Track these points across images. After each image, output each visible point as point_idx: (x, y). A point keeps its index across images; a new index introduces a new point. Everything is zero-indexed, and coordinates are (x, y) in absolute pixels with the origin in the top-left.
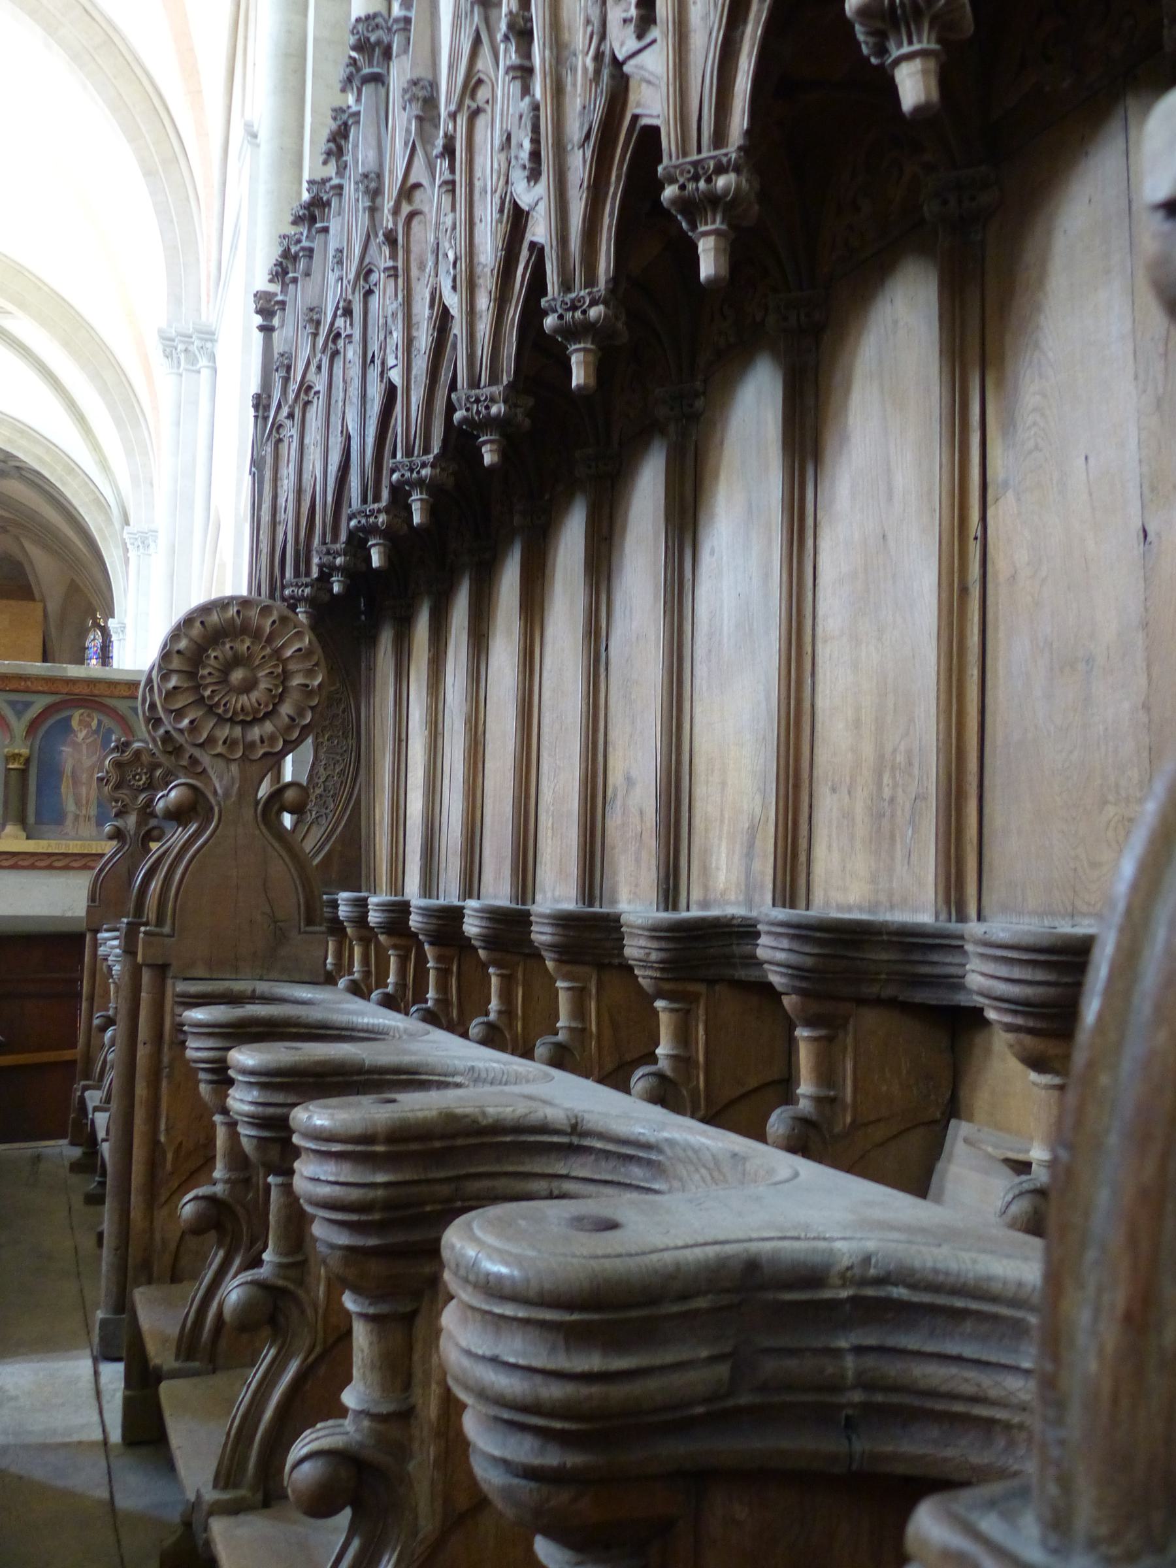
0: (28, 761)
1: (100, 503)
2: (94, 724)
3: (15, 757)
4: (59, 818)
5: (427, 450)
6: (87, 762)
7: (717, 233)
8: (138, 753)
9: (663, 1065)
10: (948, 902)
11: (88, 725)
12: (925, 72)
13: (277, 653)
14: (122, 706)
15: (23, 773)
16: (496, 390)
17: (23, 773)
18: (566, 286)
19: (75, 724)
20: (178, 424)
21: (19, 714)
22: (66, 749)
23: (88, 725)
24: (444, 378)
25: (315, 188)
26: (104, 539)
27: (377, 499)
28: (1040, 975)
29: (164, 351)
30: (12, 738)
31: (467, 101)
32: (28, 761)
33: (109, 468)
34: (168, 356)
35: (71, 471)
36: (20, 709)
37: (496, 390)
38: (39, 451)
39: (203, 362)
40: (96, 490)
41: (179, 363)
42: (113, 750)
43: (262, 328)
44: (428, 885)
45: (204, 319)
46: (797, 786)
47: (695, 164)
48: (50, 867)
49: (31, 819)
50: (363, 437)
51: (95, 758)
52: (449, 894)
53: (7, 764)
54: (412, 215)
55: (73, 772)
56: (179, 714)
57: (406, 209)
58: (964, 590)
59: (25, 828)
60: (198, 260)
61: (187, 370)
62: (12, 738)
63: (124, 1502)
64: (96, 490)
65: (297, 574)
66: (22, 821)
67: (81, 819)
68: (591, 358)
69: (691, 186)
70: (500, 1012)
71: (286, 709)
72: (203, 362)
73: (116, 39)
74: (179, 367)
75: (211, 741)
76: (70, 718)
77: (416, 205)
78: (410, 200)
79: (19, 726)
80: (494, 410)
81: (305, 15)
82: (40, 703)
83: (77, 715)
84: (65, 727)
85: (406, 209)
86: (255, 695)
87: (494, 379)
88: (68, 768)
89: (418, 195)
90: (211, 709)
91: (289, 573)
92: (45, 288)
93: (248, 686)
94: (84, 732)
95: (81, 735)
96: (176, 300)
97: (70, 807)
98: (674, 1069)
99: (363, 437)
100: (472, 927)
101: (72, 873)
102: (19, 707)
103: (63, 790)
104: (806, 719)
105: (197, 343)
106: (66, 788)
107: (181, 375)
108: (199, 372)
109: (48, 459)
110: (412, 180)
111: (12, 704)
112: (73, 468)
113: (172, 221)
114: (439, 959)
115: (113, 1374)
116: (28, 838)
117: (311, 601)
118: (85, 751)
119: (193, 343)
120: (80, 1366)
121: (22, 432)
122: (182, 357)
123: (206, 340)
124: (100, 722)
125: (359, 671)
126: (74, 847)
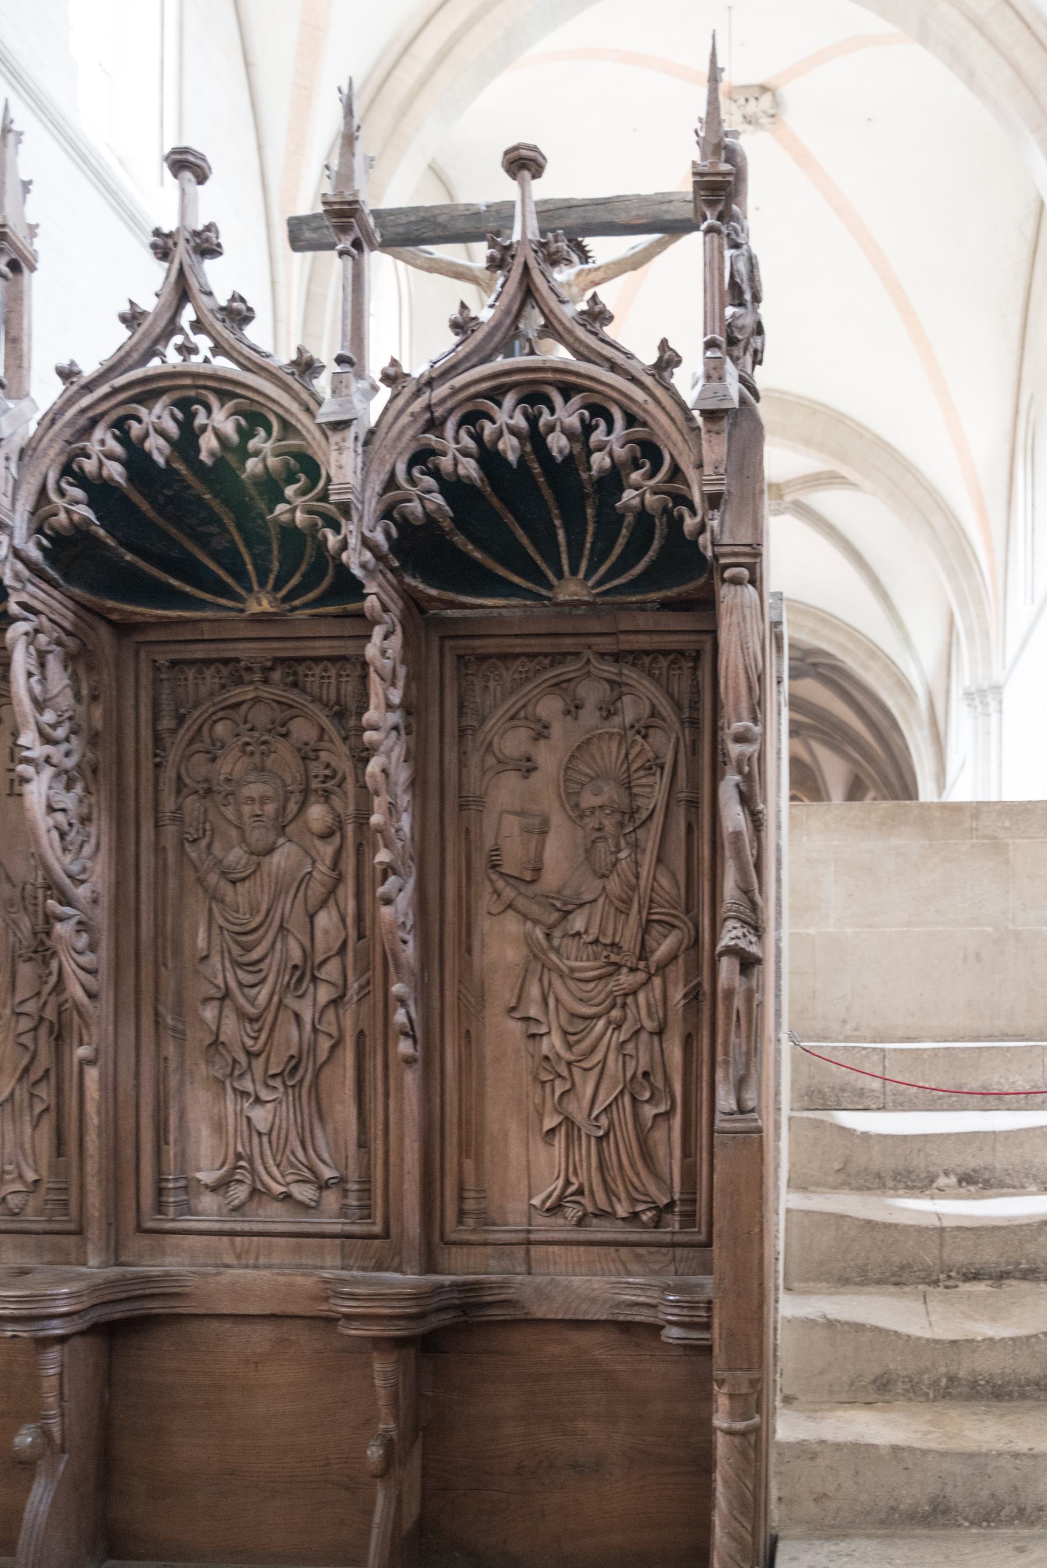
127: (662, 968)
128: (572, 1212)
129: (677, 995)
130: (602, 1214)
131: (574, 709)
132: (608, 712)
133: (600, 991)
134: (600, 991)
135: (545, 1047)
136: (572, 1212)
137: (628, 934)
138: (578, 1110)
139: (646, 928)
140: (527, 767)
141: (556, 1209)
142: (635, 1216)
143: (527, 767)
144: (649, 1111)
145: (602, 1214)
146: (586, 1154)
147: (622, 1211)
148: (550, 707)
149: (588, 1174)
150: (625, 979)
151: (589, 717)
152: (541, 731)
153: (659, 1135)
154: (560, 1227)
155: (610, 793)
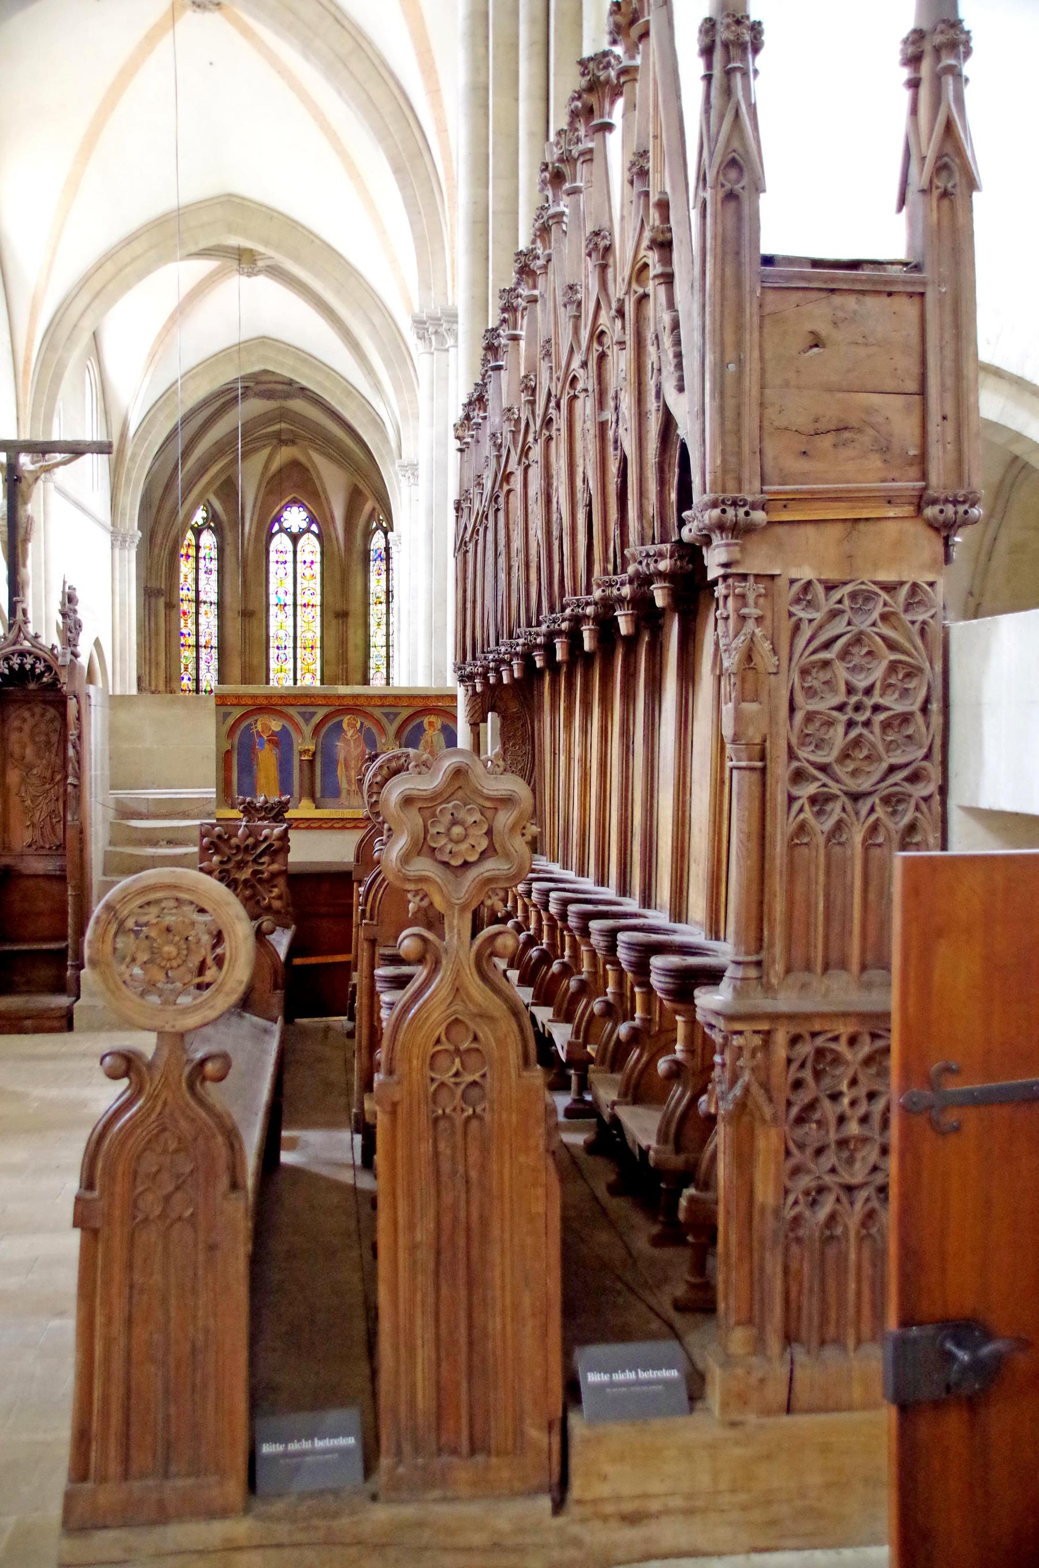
0: (314, 754)
1: (377, 423)
2: (358, 725)
4: (336, 793)
6: (355, 752)
7: (590, 630)
9: (610, 997)
10: (711, 931)
12: (626, 622)
14: (377, 712)
17: (311, 762)
18: (552, 610)
19: (345, 726)
20: (432, 398)
21: (307, 721)
22: (340, 744)
25: (479, 388)
26: (382, 457)
28: (668, 980)
29: (418, 333)
30: (303, 738)
31: (523, 460)
32: (314, 754)
34: (421, 338)
35: (349, 394)
36: (307, 717)
38: (320, 377)
39: (450, 342)
41: (431, 342)
45: (450, 303)
46: (682, 856)
47: (578, 600)
48: (332, 828)
49: (318, 795)
51: (359, 750)
53: (301, 755)
54: (509, 491)
55: (345, 759)
57: (506, 488)
58: (723, 782)
59: (314, 802)
60: (443, 247)
61: (436, 349)
62: (303, 738)
63: (359, 1185)
66: (312, 796)
67: (352, 794)
68: (565, 646)
69: (576, 610)
70: (570, 957)
73: (365, 45)
74: (431, 346)
78: (508, 482)
79: (308, 730)
80: (538, 641)
81: (487, 188)
82: (321, 713)
83: (346, 720)
84: (338, 727)
85: (506, 488)
88: (341, 757)
89: (512, 479)
92: (318, 242)
94: (352, 731)
95: (350, 733)
96: (425, 284)
97: (344, 785)
98: (615, 999)
101: (346, 831)
102: (307, 717)
103: (339, 773)
104: (687, 821)
105: (445, 326)
106: (340, 771)
107: (433, 354)
108: (447, 350)
109: (327, 384)
110: (509, 470)
111: (302, 714)
112: (351, 391)
115: (358, 1138)
116: (317, 808)
118: (352, 745)
119: (441, 325)
120: (345, 1135)
121: (305, 360)
122: (433, 337)
124: (362, 724)
125: (533, 696)
126: (347, 814)
127: (57, 783)
128: (34, 847)
129: (61, 790)
130: (42, 847)
131: (33, 715)
132: (43, 715)
133: (41, 789)
134: (41, 789)
135: (26, 804)
136: (34, 847)
137: (48, 774)
138: (35, 819)
139: (53, 772)
140: (20, 730)
141: (30, 846)
142: (50, 848)
143: (20, 730)
144: (54, 820)
145: (42, 847)
146: (38, 832)
147: (47, 846)
148: (27, 714)
149: (38, 837)
150: (47, 786)
151: (37, 717)
152: (24, 720)
153: (57, 827)
154: (31, 851)
155: (43, 738)
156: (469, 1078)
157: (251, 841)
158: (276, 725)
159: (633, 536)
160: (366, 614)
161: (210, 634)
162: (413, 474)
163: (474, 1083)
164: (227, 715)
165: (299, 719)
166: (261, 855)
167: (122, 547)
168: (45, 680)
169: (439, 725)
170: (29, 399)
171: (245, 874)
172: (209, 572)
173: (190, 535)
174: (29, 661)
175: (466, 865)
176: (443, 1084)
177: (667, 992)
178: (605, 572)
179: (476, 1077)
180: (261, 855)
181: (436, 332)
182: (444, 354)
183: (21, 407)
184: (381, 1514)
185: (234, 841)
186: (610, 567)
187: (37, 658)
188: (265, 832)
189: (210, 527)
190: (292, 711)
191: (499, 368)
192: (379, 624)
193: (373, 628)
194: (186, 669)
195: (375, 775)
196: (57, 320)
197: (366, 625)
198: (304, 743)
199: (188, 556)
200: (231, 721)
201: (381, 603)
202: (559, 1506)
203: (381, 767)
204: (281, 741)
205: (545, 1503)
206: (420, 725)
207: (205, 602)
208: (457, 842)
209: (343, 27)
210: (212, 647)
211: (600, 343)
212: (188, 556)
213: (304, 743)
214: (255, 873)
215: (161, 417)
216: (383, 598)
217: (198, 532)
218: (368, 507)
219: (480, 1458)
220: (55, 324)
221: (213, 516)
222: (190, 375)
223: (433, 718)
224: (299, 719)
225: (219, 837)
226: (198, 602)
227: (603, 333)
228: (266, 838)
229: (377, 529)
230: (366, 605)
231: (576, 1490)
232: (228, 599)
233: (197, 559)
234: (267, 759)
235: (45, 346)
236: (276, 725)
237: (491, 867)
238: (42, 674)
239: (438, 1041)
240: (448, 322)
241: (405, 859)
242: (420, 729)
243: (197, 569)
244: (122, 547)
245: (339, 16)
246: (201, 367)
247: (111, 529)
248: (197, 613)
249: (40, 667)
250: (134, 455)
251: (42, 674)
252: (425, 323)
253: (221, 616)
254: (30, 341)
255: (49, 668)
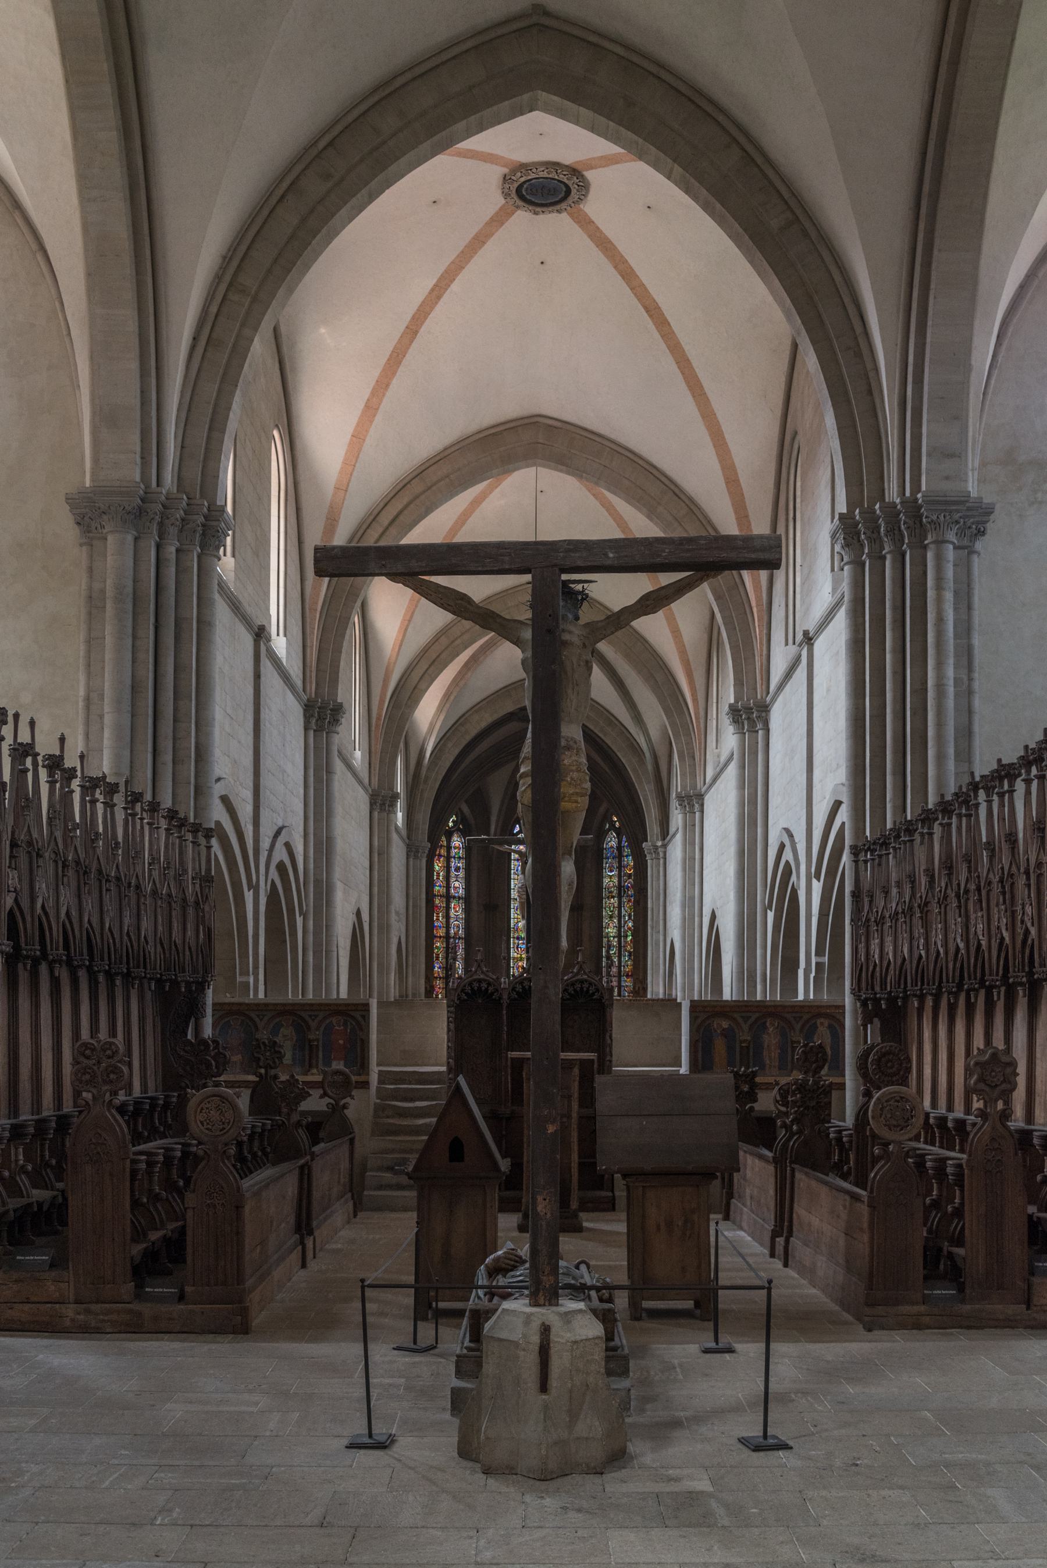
1: (635, 748)
2: (776, 1024)
3: (745, 1041)
5: (934, 984)
8: (812, 1046)
11: (774, 1025)
13: (899, 1059)
15: (748, 1047)
16: (955, 985)
17: (748, 1047)
18: (970, 979)
19: (768, 1024)
21: (745, 1022)
23: (774, 1025)
24: (939, 965)
27: (916, 985)
29: (733, 719)
33: (642, 720)
37: (955, 985)
39: (759, 726)
40: (631, 738)
42: (802, 1047)
43: (854, 861)
44: (934, 1104)
45: (759, 697)
50: (911, 969)
52: (942, 1110)
54: (927, 911)
56: (876, 1075)
64: (631, 738)
65: (882, 990)
71: (901, 1073)
72: (759, 726)
74: (743, 728)
75: (884, 1081)
76: (766, 1022)
77: (929, 908)
79: (745, 1027)
82: (754, 1016)
85: (925, 909)
86: (894, 1069)
87: (953, 982)
88: (766, 1046)
90: (883, 1073)
91: (877, 989)
93: (891, 1067)
99: (911, 969)
100: (950, 1125)
108: (757, 732)
113: (735, 628)
114: (940, 1133)
117: (887, 1000)
122: (746, 722)
123: (762, 711)
156: (997, 1158)
157: (815, 1087)
158: (725, 1024)
159: (1036, 965)
160: (599, 908)
161: (458, 927)
162: (689, 804)
163: (999, 1160)
164: (696, 1018)
165: (740, 1020)
166: (820, 1095)
167: (416, 857)
168: (595, 997)
169: (826, 1024)
170: (379, 747)
171: (813, 1103)
172: (457, 869)
173: (444, 838)
174: (586, 985)
175: (996, 1086)
176: (989, 1160)
177: (1040, 1145)
178: (1014, 972)
179: (1000, 1158)
180: (820, 1095)
181: (748, 719)
182: (754, 734)
183: (373, 755)
184: (967, 1308)
185: (807, 1087)
186: (1016, 970)
187: (591, 984)
188: (822, 1083)
189: (459, 830)
190: (736, 1015)
191: (913, 840)
192: (611, 917)
193: (606, 921)
194: (437, 958)
195: (874, 1056)
196: (402, 683)
197: (599, 918)
198: (744, 1035)
199: (440, 856)
200: (699, 1021)
201: (613, 897)
202: (1028, 1308)
203: (877, 1052)
204: (729, 1035)
205: (1024, 1306)
206: (815, 1023)
207: (454, 897)
208: (994, 1077)
209: (679, 498)
210: (459, 938)
211: (1012, 878)
212: (440, 856)
213: (744, 1035)
214: (817, 1103)
215: (450, 745)
216: (615, 893)
217: (449, 835)
218: (602, 809)
219: (1000, 1291)
220: (400, 686)
221: (462, 819)
222: (476, 708)
223: (822, 1020)
224: (740, 1020)
225: (801, 1085)
226: (448, 897)
227: (1013, 874)
228: (823, 1086)
229: (609, 830)
230: (599, 899)
231: (1035, 1300)
232: (474, 895)
233: (448, 858)
234: (720, 1046)
235: (391, 705)
236: (725, 1024)
237: (1004, 1086)
238: (593, 994)
239: (987, 1145)
240: (757, 711)
241: (976, 1083)
242: (815, 1027)
243: (448, 868)
244: (416, 857)
245: (676, 490)
246: (484, 702)
247: (407, 841)
248: (448, 908)
249: (592, 990)
250: (427, 778)
251: (593, 994)
252: (740, 711)
253: (467, 910)
254: (382, 701)
255: (597, 990)
